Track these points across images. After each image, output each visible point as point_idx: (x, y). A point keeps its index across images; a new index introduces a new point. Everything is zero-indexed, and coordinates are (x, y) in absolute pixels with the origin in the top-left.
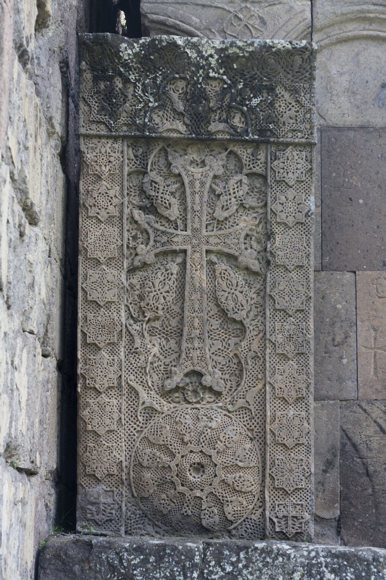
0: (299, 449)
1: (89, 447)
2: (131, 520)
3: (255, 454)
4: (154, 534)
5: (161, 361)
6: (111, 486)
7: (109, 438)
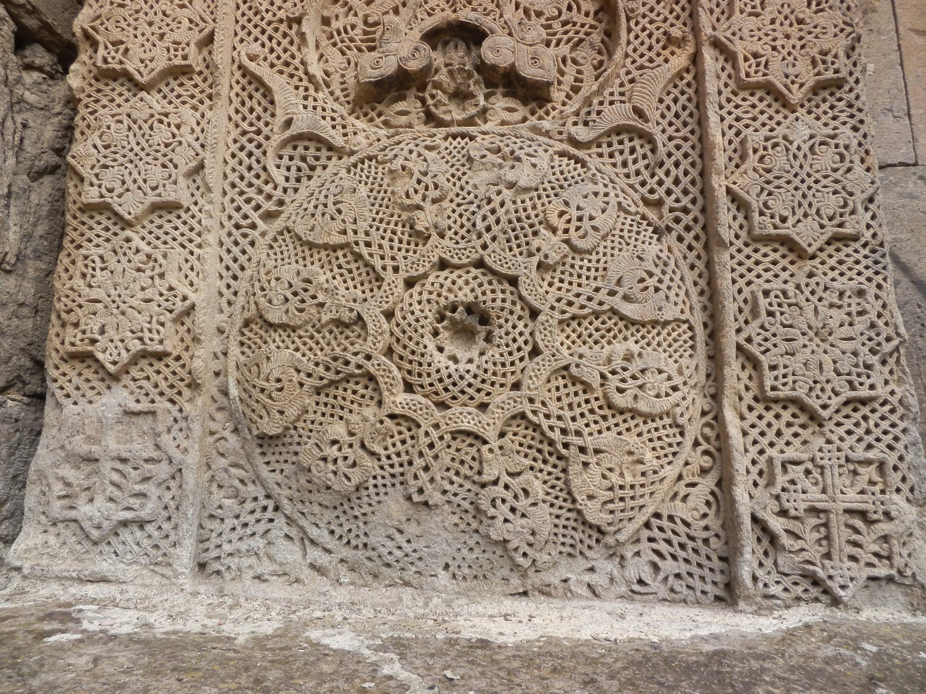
0: (842, 255)
1: (86, 258)
2: (222, 520)
3: (677, 278)
4: (306, 573)
5: (356, 15)
6: (153, 392)
7: (160, 233)
